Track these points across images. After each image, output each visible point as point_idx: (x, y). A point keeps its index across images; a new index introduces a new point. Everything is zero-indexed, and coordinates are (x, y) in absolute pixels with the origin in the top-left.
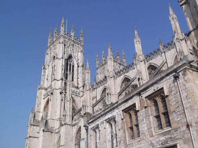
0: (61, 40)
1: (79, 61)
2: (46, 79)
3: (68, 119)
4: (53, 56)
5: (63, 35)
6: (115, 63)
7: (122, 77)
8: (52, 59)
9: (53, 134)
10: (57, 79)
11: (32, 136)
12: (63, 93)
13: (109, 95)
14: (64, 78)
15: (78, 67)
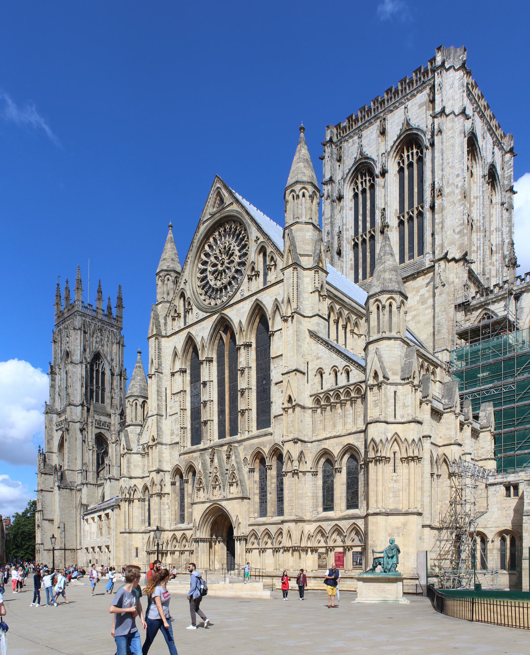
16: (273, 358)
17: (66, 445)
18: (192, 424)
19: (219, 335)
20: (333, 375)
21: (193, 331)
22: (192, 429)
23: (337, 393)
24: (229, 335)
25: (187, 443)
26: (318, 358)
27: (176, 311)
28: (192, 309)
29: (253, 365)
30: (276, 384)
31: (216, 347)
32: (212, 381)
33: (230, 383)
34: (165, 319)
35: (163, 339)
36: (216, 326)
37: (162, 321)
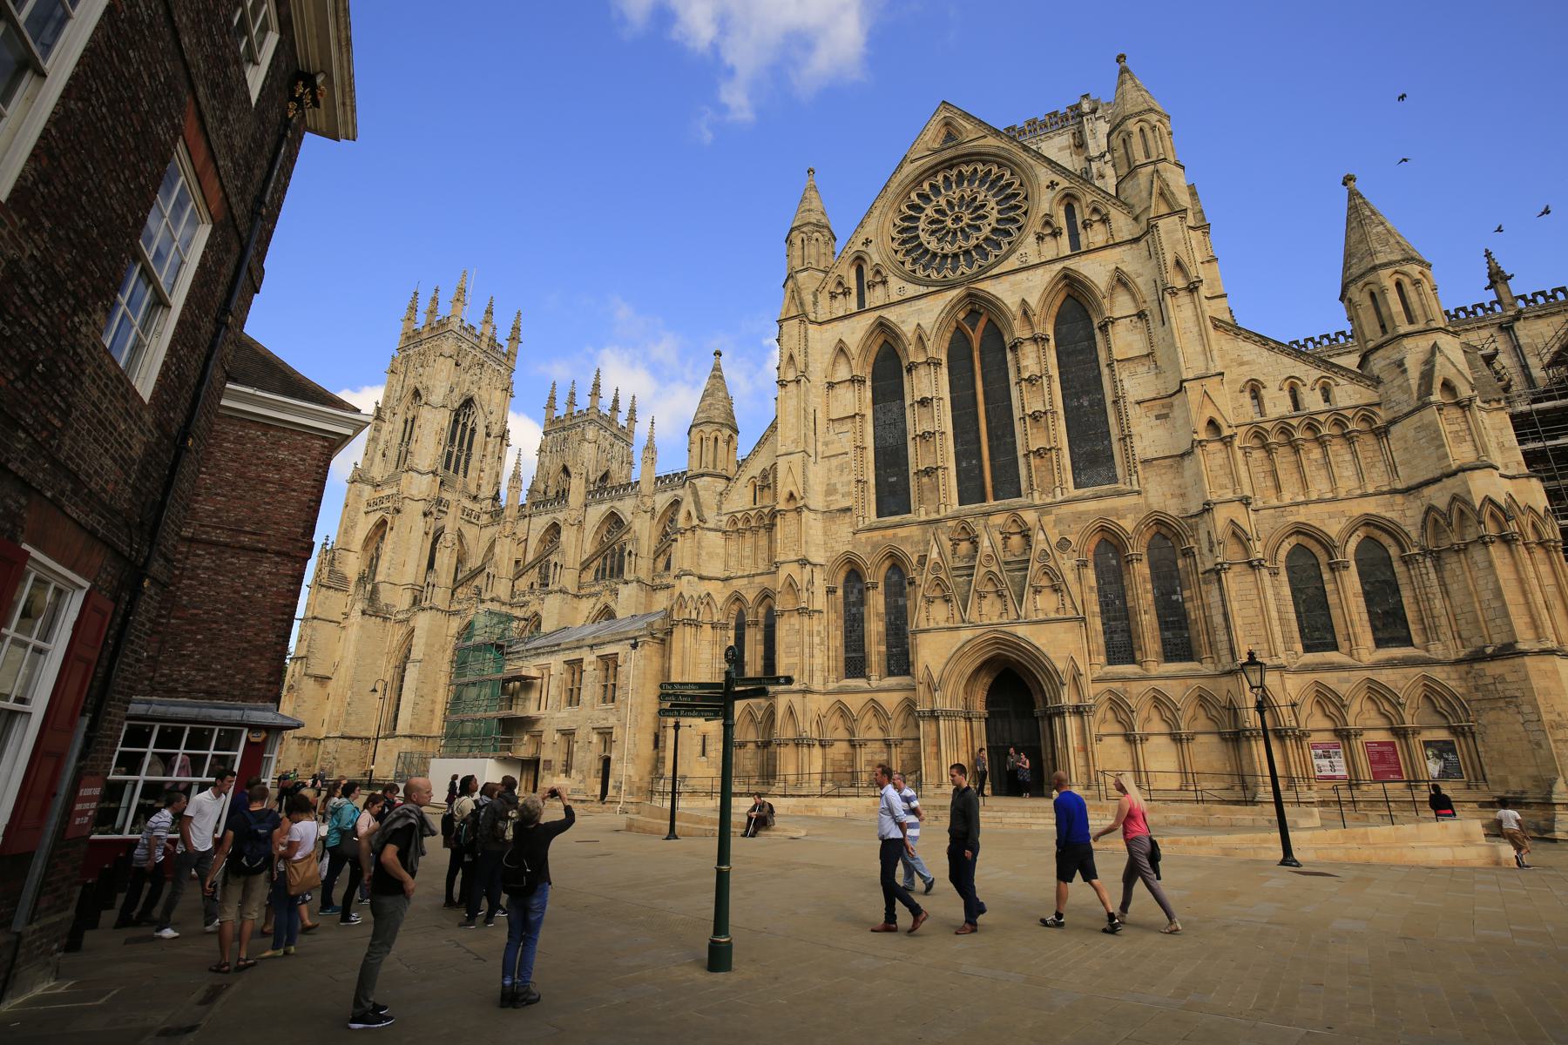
0: (448, 346)
1: (492, 418)
2: (380, 453)
3: (440, 595)
4: (413, 387)
5: (457, 329)
6: (601, 432)
7: (604, 508)
8: (409, 396)
9: (388, 624)
10: (420, 468)
11: (319, 616)
12: (431, 513)
13: (559, 568)
14: (439, 470)
15: (488, 435)
16: (1118, 361)
17: (387, 547)
18: (877, 476)
19: (954, 324)
20: (1286, 393)
21: (892, 315)
22: (877, 484)
23: (1309, 423)
24: (981, 324)
25: (869, 511)
26: (1242, 364)
27: (840, 284)
28: (884, 282)
29: (1055, 373)
30: (1139, 403)
31: (947, 346)
32: (942, 399)
33: (986, 403)
34: (815, 296)
35: (810, 326)
36: (953, 307)
37: (808, 298)
